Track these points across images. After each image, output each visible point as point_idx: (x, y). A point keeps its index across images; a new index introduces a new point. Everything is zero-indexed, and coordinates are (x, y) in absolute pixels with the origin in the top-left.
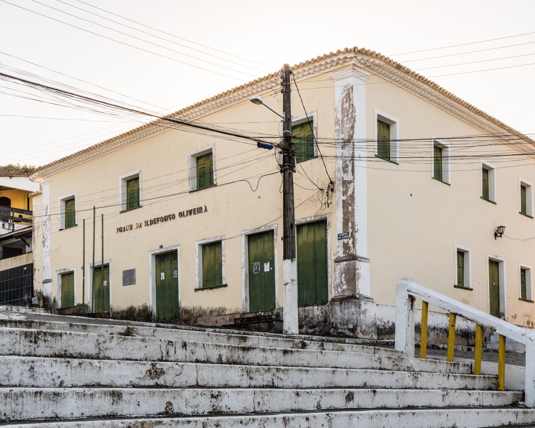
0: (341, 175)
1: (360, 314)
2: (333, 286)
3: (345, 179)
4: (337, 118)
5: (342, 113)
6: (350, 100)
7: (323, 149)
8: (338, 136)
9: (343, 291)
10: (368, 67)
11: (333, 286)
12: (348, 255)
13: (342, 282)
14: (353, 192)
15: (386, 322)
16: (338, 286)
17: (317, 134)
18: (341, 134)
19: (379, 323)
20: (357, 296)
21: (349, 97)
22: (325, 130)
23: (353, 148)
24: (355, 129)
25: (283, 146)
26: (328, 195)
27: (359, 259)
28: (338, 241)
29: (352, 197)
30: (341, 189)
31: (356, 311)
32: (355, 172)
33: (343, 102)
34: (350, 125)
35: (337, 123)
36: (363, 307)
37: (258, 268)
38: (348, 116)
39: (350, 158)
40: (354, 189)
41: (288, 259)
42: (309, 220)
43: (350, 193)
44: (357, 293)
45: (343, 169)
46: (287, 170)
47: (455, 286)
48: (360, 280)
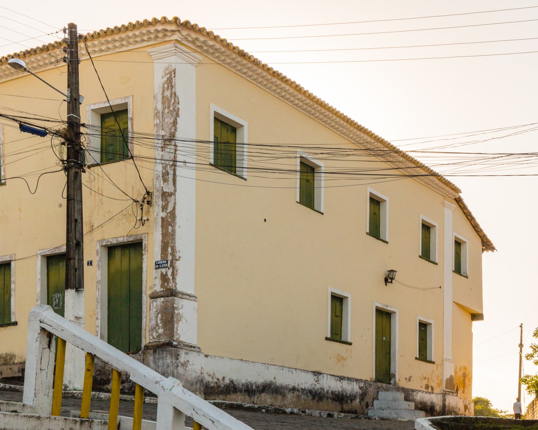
0: (160, 184)
1: (178, 366)
2: (148, 329)
3: (165, 190)
4: (156, 109)
5: (163, 103)
6: (172, 87)
7: (137, 149)
8: (157, 132)
9: (159, 336)
10: (200, 47)
11: (148, 329)
12: (167, 289)
13: (157, 325)
14: (174, 209)
15: (221, 379)
16: (153, 329)
17: (132, 127)
18: (160, 131)
19: (208, 379)
20: (175, 343)
21: (171, 83)
22: (142, 122)
23: (176, 150)
24: (178, 126)
25: (65, 135)
26: (142, 209)
27: (181, 296)
28: (155, 271)
29: (173, 214)
30: (160, 203)
31: (172, 362)
32: (178, 182)
33: (163, 88)
34: (172, 120)
35: (156, 115)
36: (183, 357)
37: (59, 302)
38: (169, 108)
39: (171, 163)
40: (175, 203)
41: (71, 288)
42: (121, 240)
43: (170, 209)
44: (175, 339)
45: (163, 177)
46: (71, 168)
47: (327, 339)
48: (180, 322)
